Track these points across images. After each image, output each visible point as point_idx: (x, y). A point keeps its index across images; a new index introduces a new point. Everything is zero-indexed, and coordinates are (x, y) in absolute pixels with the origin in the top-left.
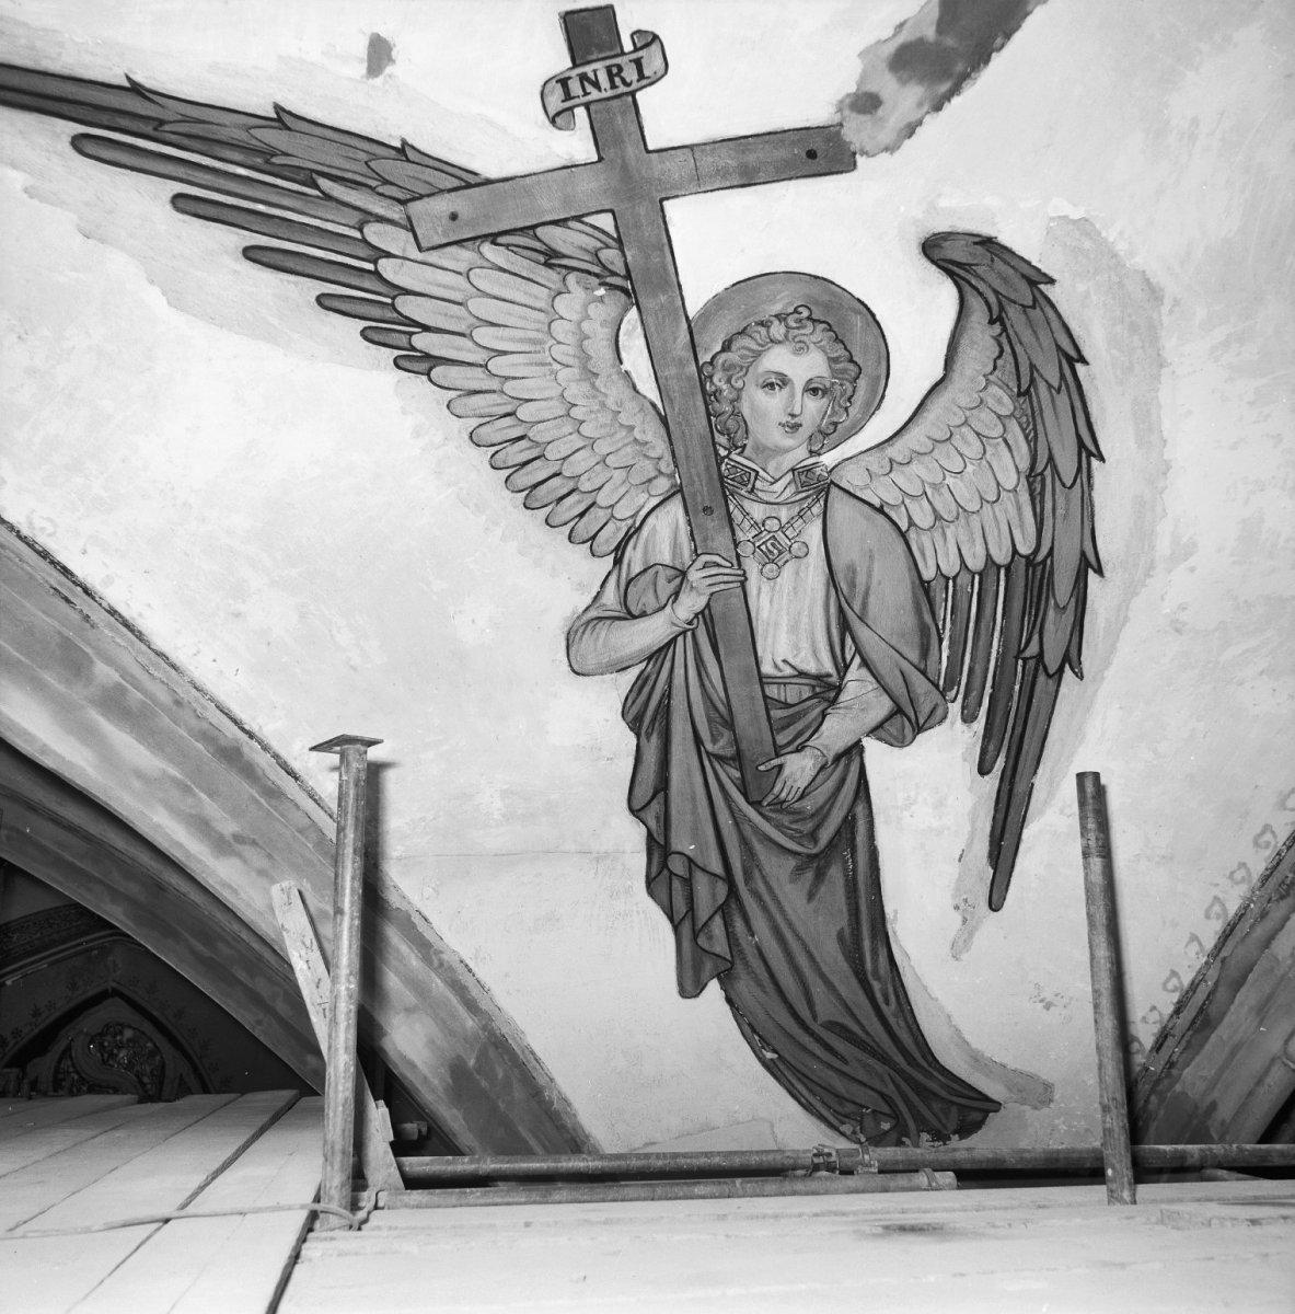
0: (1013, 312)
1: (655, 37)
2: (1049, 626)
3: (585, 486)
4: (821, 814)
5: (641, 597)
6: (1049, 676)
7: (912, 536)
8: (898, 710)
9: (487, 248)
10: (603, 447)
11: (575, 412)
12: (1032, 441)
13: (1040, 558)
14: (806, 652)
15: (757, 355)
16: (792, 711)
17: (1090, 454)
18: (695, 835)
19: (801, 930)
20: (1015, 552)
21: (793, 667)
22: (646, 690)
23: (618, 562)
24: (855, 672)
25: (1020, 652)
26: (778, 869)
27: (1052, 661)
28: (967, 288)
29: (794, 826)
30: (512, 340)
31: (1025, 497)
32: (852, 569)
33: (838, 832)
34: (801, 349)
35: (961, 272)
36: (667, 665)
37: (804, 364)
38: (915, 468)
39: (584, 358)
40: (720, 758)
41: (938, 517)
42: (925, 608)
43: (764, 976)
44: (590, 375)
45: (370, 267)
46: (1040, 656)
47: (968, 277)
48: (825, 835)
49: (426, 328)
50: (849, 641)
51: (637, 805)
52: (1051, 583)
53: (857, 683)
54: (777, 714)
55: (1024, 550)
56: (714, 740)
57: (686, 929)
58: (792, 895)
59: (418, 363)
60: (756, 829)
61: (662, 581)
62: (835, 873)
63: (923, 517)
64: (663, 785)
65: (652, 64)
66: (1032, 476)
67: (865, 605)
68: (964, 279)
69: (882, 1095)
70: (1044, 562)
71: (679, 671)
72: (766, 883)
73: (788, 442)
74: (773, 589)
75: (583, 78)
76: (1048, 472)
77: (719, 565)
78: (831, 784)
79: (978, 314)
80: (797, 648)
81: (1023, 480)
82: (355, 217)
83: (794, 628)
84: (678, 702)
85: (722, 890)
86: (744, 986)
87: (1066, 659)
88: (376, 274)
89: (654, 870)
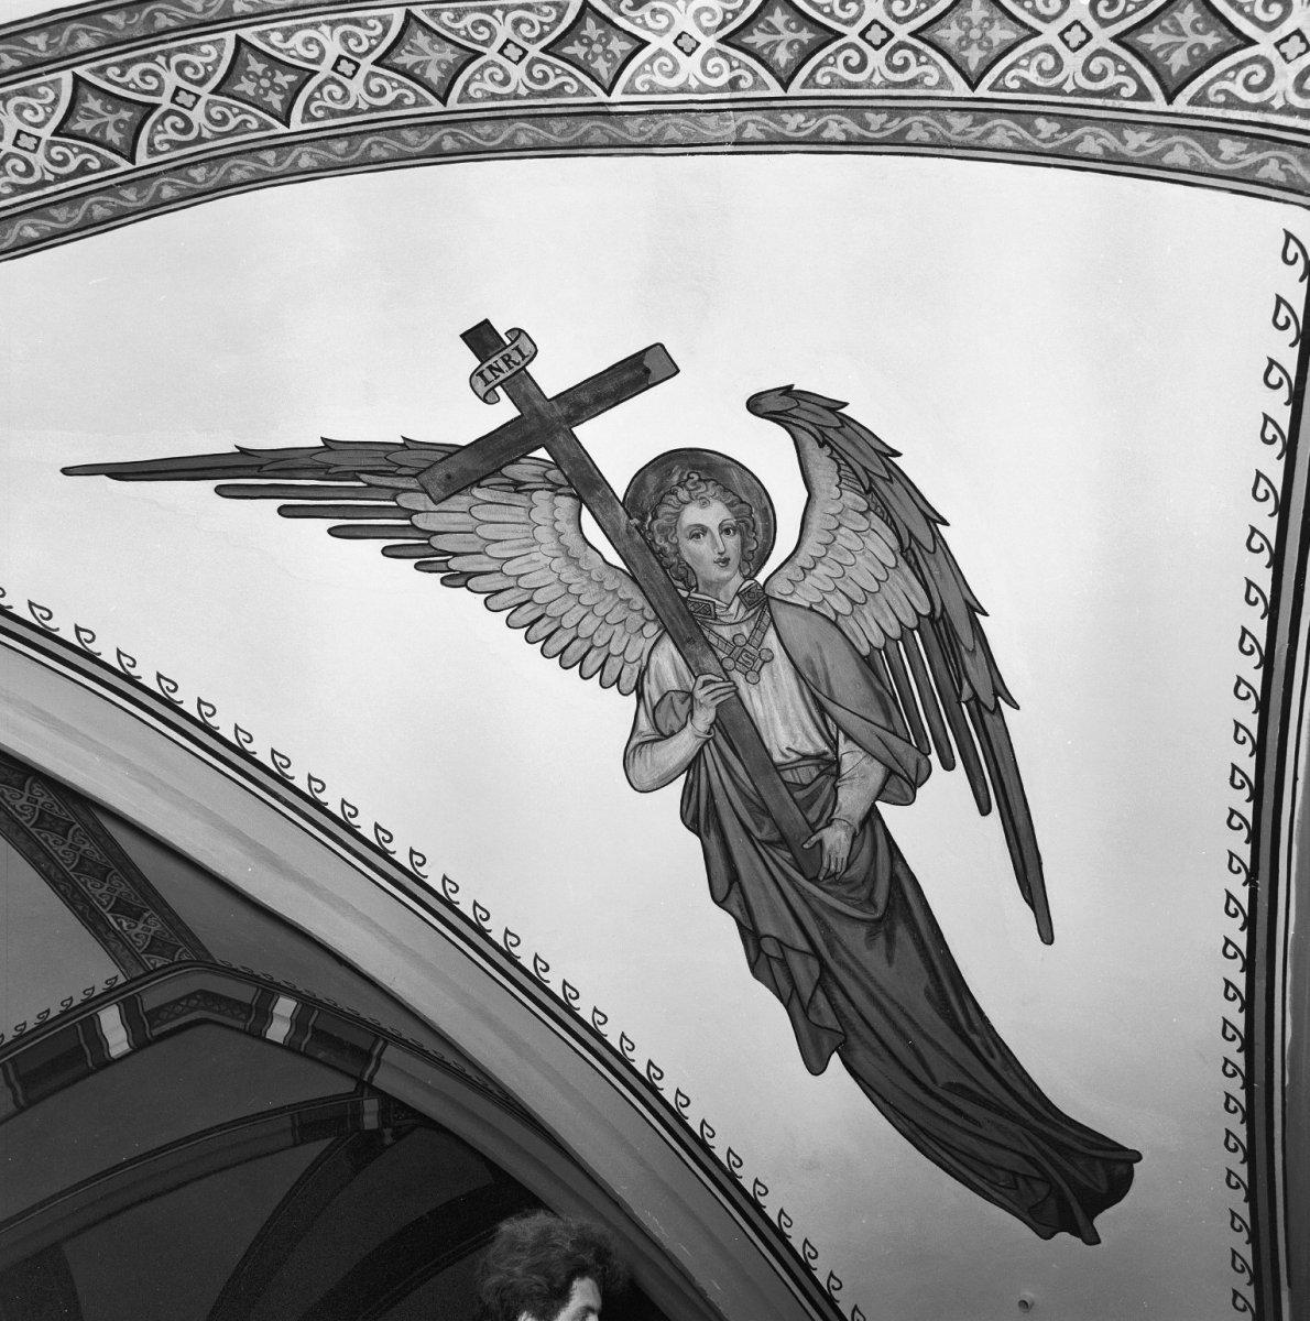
0: (831, 433)
1: (520, 331)
2: (970, 669)
3: (598, 642)
4: (870, 878)
5: (668, 721)
6: (992, 713)
7: (841, 621)
8: (890, 773)
9: (476, 492)
10: (600, 610)
11: (573, 589)
12: (892, 525)
13: (938, 615)
14: (801, 738)
15: (678, 515)
16: (810, 789)
18: (776, 918)
19: (894, 994)
20: (919, 615)
21: (797, 752)
22: (694, 795)
23: (640, 696)
24: (844, 746)
26: (853, 937)
27: (986, 697)
28: (792, 427)
29: (852, 895)
30: (513, 548)
31: (907, 570)
32: (809, 661)
33: (890, 895)
34: (705, 503)
35: (782, 417)
36: (703, 769)
37: (713, 514)
38: (821, 570)
39: (566, 550)
40: (770, 843)
41: (853, 603)
42: (874, 679)
43: (876, 1044)
44: (573, 560)
45: (407, 522)
46: (976, 697)
47: (790, 419)
48: (881, 898)
49: (455, 555)
50: (829, 721)
51: (720, 898)
52: (955, 634)
53: (850, 757)
54: (799, 795)
55: (925, 611)
56: (760, 829)
57: (796, 1005)
58: (873, 959)
59: (456, 579)
60: (821, 902)
61: (677, 704)
62: (901, 932)
63: (845, 608)
64: (734, 877)
65: (527, 349)
66: (904, 551)
68: (787, 422)
69: (1026, 1157)
70: (942, 617)
71: (714, 775)
72: (848, 952)
73: (725, 574)
74: (759, 691)
75: (490, 368)
76: (914, 545)
77: (715, 682)
78: (866, 850)
79: (810, 445)
80: (792, 735)
81: (899, 556)
82: (389, 493)
83: (786, 720)
84: (721, 801)
85: (814, 965)
86: (861, 1056)
87: (996, 694)
88: (413, 526)
89: (753, 959)
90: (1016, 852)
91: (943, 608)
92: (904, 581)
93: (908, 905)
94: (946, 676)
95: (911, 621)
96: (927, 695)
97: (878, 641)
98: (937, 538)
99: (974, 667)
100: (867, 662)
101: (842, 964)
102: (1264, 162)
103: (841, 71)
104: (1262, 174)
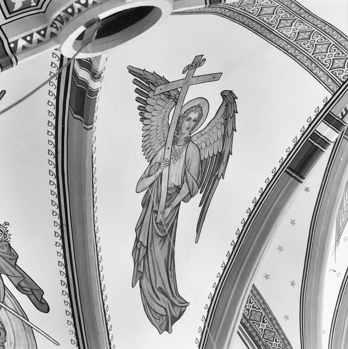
6: (218, 179)
8: (190, 193)
12: (225, 128)
13: (222, 153)
16: (171, 196)
17: (234, 130)
20: (218, 152)
24: (185, 184)
25: (215, 174)
31: (222, 140)
32: (189, 159)
35: (225, 97)
38: (205, 136)
41: (206, 145)
42: (200, 166)
47: (226, 99)
50: (185, 177)
52: (223, 158)
55: (220, 151)
60: (155, 230)
62: (167, 242)
63: (203, 147)
64: (142, 223)
67: (189, 168)
68: (225, 99)
69: (165, 309)
70: (223, 154)
71: (154, 189)
74: (174, 166)
76: (226, 135)
78: (172, 215)
79: (224, 105)
80: (175, 180)
81: (222, 136)
83: (176, 175)
86: (145, 281)
87: (222, 175)
90: (200, 217)
91: (224, 152)
92: (220, 143)
93: (172, 232)
94: (215, 168)
95: (215, 153)
96: (209, 173)
97: (206, 158)
98: (232, 134)
99: (222, 167)
100: (201, 162)
101: (151, 251)
102: (332, 85)
103: (302, 43)
104: (330, 87)
